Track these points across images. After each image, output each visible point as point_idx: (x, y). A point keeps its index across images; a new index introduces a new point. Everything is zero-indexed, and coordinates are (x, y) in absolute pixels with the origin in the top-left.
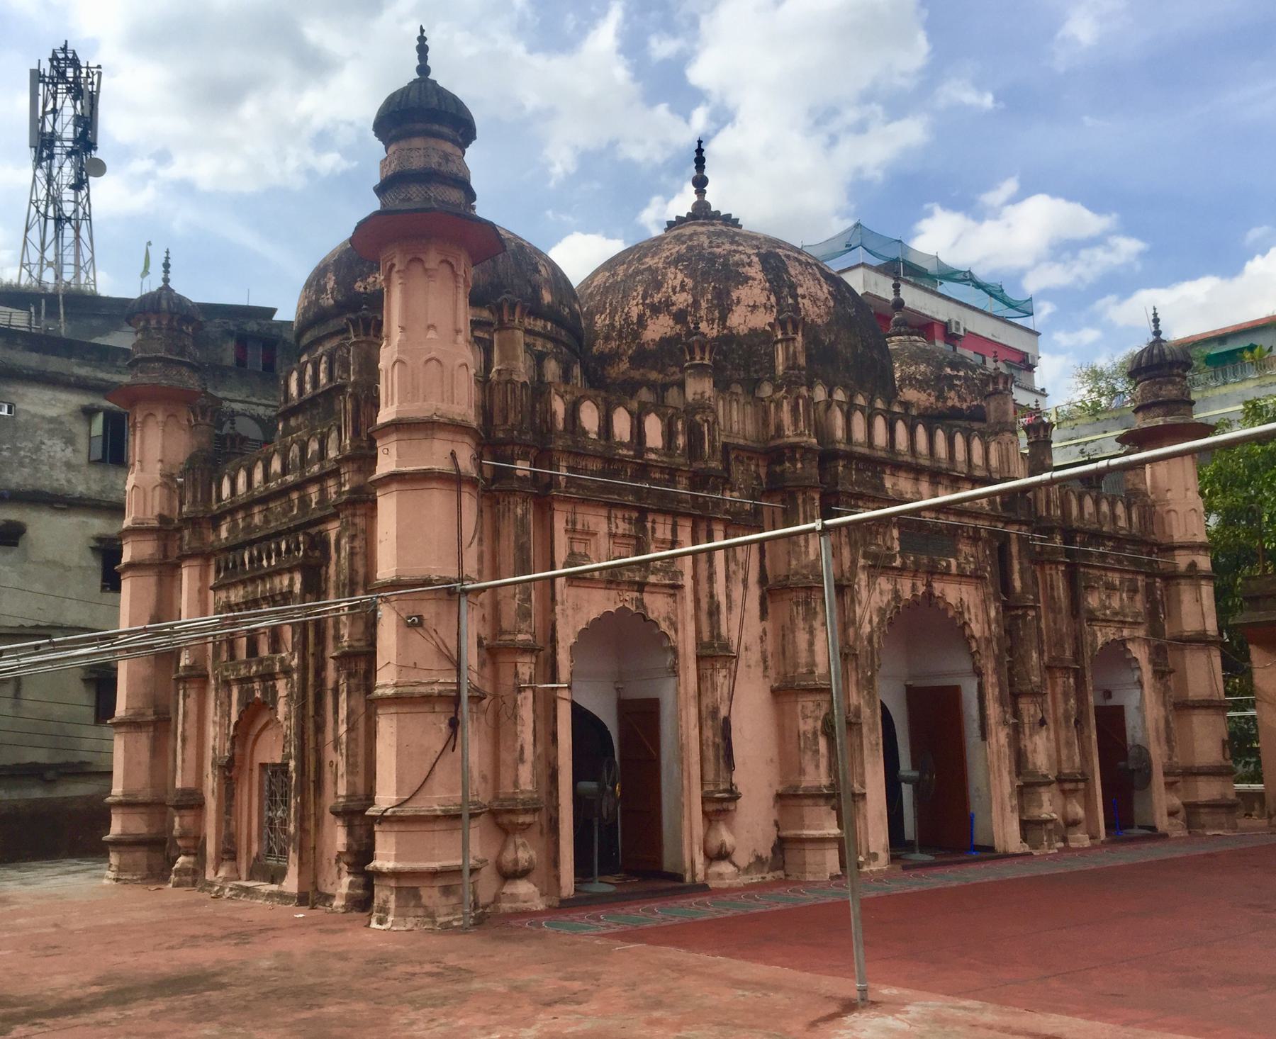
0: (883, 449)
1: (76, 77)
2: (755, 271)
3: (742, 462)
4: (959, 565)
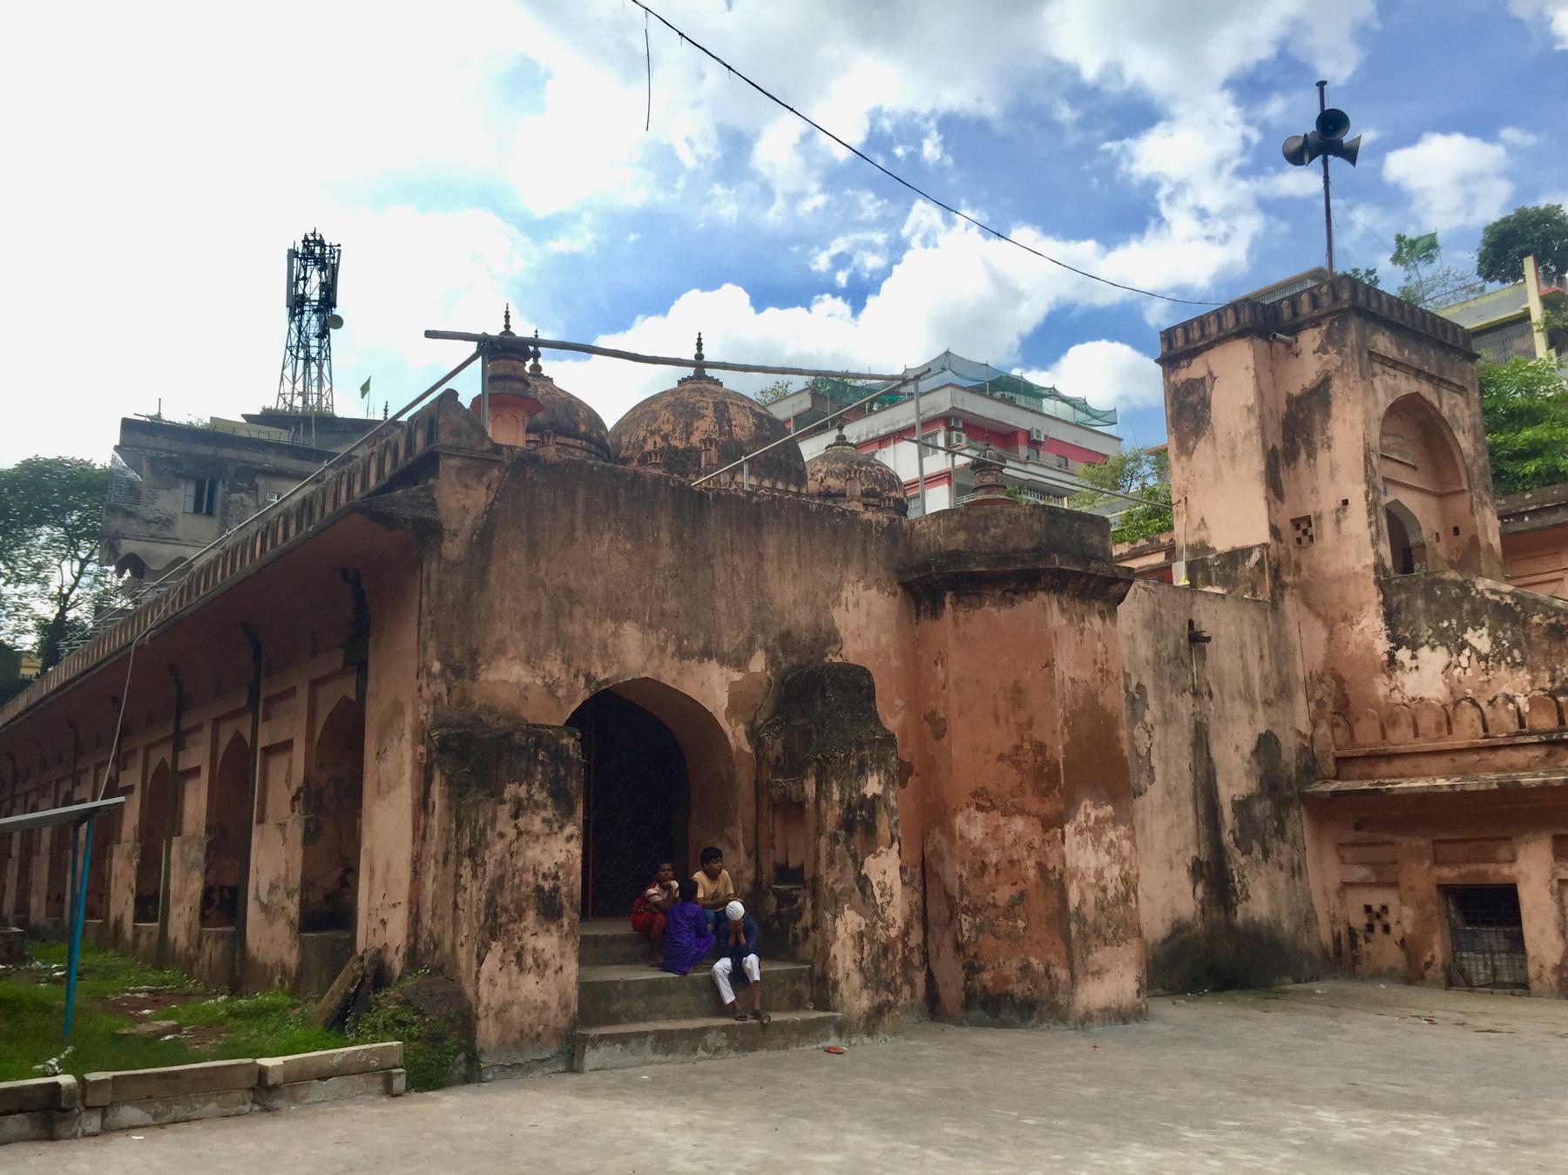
1: (322, 254)
2: (709, 412)
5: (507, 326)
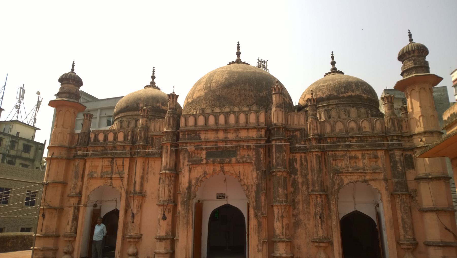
0: (202, 126)
3: (158, 139)
4: (236, 159)
5: (73, 70)
